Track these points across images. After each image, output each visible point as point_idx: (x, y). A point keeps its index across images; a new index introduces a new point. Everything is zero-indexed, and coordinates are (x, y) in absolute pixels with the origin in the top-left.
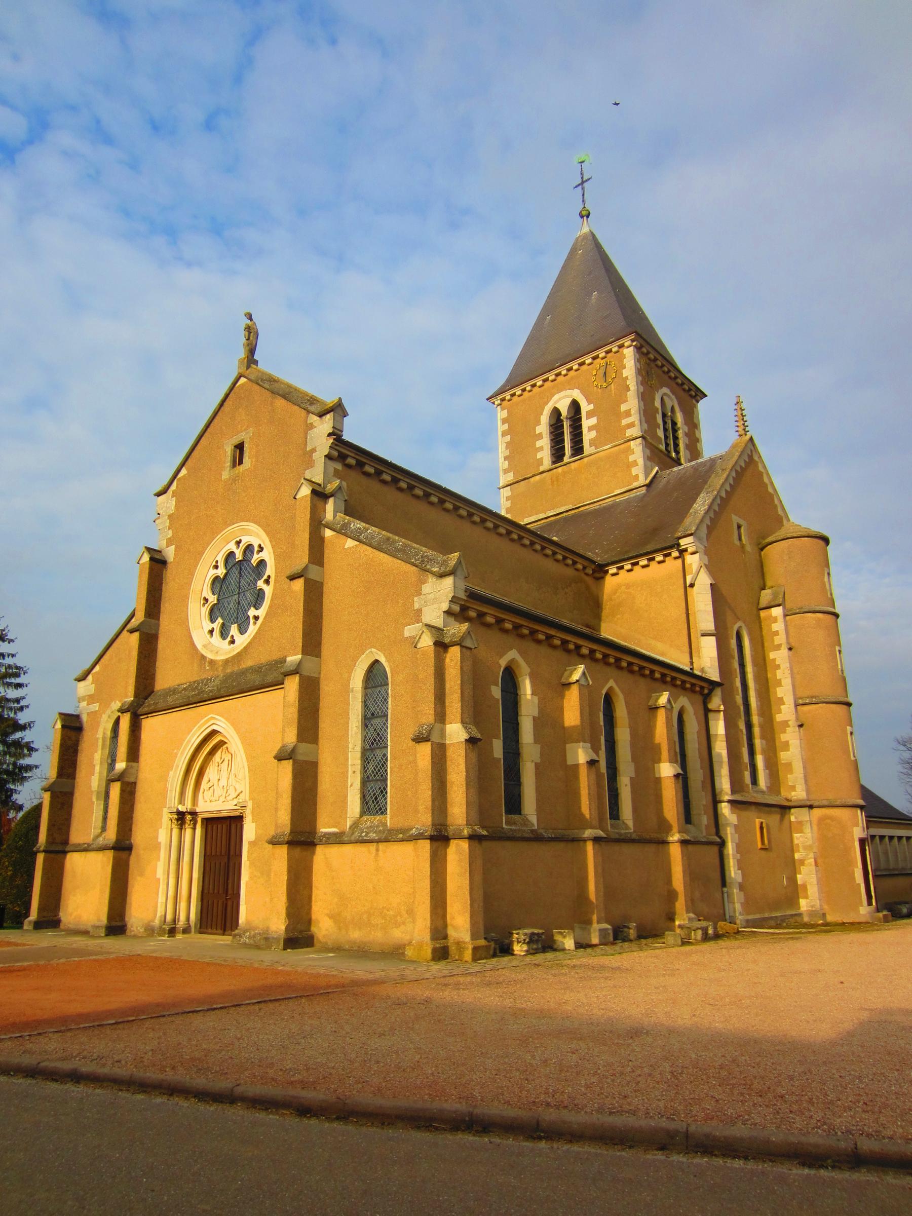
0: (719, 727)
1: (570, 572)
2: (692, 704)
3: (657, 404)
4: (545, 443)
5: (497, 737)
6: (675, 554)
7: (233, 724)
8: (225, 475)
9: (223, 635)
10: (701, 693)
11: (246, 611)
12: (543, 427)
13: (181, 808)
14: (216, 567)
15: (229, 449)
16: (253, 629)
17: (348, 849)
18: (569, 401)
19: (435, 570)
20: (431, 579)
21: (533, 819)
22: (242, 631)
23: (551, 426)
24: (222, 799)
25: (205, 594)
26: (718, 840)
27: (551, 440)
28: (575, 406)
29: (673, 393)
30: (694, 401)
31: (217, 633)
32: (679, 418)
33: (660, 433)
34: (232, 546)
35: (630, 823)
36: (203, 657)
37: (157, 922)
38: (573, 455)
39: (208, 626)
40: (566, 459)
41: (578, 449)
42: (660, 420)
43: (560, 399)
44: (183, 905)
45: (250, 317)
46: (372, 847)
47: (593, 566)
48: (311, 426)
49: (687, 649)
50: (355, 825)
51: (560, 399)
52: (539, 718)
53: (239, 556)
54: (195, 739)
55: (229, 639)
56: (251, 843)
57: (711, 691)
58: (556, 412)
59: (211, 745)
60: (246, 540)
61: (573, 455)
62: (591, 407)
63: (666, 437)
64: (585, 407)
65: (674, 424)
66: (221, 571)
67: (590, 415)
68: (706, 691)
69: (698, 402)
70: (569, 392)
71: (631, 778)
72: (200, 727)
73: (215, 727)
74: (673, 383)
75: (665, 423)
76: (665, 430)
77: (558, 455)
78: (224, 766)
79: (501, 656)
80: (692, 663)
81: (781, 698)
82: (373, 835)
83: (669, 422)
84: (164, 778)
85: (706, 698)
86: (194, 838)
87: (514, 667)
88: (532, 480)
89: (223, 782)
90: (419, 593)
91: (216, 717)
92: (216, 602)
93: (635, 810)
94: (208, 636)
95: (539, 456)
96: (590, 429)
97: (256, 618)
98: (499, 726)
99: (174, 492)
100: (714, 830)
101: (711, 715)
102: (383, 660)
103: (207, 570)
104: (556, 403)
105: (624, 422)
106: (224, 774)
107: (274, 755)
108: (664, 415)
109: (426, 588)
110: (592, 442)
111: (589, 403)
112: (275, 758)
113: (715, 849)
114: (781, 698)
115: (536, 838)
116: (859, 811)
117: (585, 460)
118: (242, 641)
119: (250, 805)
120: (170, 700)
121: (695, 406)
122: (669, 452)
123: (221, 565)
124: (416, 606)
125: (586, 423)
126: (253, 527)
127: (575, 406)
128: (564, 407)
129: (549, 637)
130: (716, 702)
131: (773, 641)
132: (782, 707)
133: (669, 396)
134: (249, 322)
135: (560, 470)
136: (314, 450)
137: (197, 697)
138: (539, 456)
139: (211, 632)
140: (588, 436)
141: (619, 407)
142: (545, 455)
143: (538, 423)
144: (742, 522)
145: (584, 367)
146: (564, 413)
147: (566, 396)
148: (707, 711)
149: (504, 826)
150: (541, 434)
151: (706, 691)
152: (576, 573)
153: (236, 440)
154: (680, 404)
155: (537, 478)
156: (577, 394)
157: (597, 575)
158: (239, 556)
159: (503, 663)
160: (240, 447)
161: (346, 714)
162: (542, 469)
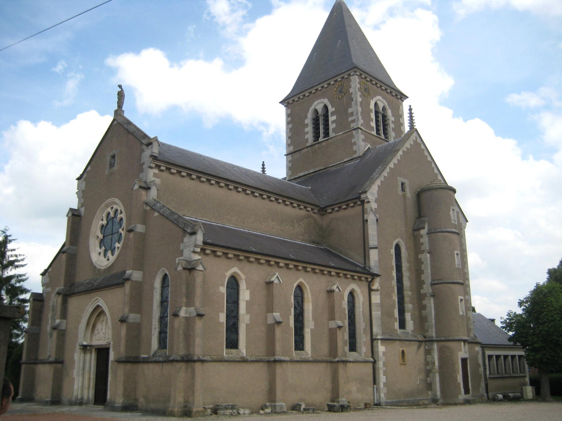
0: (376, 298)
1: (303, 212)
2: (360, 287)
3: (372, 107)
4: (310, 129)
5: (222, 312)
6: (359, 203)
7: (106, 302)
8: (107, 172)
9: (105, 256)
10: (367, 281)
11: (115, 243)
12: (309, 121)
13: (85, 343)
14: (102, 220)
15: (109, 158)
16: (117, 252)
17: (151, 366)
18: (322, 105)
19: (189, 231)
20: (187, 235)
21: (244, 352)
22: (113, 255)
23: (313, 119)
24: (103, 339)
25: (97, 234)
26: (372, 360)
27: (314, 128)
28: (326, 107)
29: (384, 98)
30: (400, 101)
31: (102, 254)
32: (389, 113)
33: (373, 124)
34: (109, 210)
35: (310, 352)
36: (95, 267)
37: (74, 399)
38: (324, 137)
39: (98, 250)
40: (321, 139)
41: (327, 134)
42: (373, 116)
43: (318, 104)
44: (86, 391)
45: (120, 86)
46: (160, 365)
47: (318, 208)
48: (143, 151)
49: (363, 255)
50: (154, 355)
51: (318, 104)
52: (250, 301)
53: (112, 215)
54: (91, 310)
55: (107, 258)
56: (112, 361)
57: (372, 279)
58: (316, 111)
59: (98, 313)
60: (115, 207)
61: (324, 137)
62: (333, 109)
63: (377, 125)
64: (331, 109)
65: (384, 116)
66: (105, 222)
67: (333, 114)
68: (369, 280)
69: (403, 101)
70: (322, 100)
71: (311, 329)
72: (92, 303)
73: (99, 303)
74: (384, 93)
75: (377, 117)
76: (377, 121)
77: (316, 136)
78: (104, 322)
79: (227, 271)
80: (365, 264)
81: (424, 281)
82: (161, 359)
83: (381, 116)
84: (77, 328)
85: (370, 284)
86: (92, 358)
87: (236, 276)
88: (302, 151)
89: (104, 331)
90: (182, 242)
91: (100, 300)
92: (102, 238)
93: (313, 346)
94: (98, 255)
95: (306, 137)
96: (333, 122)
97: (118, 248)
98: (224, 306)
99: (85, 178)
100: (370, 355)
101: (372, 293)
102: (168, 274)
103: (98, 223)
104: (316, 106)
105: (350, 119)
106: (104, 327)
107: (119, 319)
108: (377, 113)
109: (186, 239)
110: (334, 130)
111: (333, 107)
112: (119, 321)
113: (371, 365)
114: (424, 281)
115: (244, 361)
116: (462, 343)
117: (330, 141)
118: (112, 258)
119: (112, 343)
120: (80, 289)
121: (401, 104)
122: (379, 134)
123: (105, 219)
124: (181, 248)
125: (332, 119)
126: (117, 201)
127: (326, 107)
128: (320, 108)
129: (257, 260)
130: (376, 285)
131: (420, 248)
132: (424, 286)
133: (381, 101)
134: (120, 90)
135: (317, 146)
136: (143, 164)
137: (92, 289)
138: (306, 137)
139: (100, 254)
140: (332, 126)
141: (348, 110)
142: (310, 137)
143: (306, 118)
144: (406, 181)
145: (331, 86)
146: (320, 111)
147: (322, 103)
148: (370, 290)
149: (225, 355)
150: (307, 124)
151: (369, 280)
152: (307, 213)
153: (111, 154)
154: (389, 104)
155: (305, 150)
156: (326, 101)
157: (321, 213)
158: (112, 215)
159: (228, 274)
160: (113, 157)
161: (152, 299)
162: (308, 145)
